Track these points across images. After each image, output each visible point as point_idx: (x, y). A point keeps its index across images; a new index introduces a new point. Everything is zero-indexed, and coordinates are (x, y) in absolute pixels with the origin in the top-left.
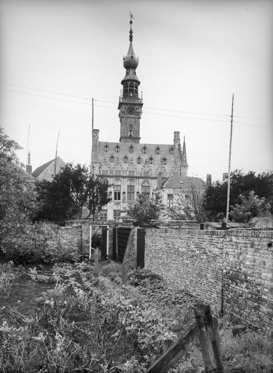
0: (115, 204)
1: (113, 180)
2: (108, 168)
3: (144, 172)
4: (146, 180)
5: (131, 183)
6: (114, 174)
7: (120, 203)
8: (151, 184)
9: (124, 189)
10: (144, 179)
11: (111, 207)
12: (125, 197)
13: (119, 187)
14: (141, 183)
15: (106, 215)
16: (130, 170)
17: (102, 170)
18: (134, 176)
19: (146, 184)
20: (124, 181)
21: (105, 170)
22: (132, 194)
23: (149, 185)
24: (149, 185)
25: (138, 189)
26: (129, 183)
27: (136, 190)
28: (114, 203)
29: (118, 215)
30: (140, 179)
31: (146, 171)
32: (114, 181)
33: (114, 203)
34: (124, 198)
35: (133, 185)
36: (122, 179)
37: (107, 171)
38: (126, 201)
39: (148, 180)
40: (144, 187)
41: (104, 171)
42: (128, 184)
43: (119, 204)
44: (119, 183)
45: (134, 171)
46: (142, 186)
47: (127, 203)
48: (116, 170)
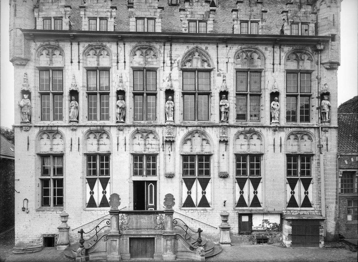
0: (91, 132)
1: (82, 49)
2: (62, 10)
3: (190, 21)
4: (197, 49)
5: (146, 62)
6: (85, 27)
7: (106, 129)
8: (216, 63)
9: (121, 81)
10: (191, 46)
11: (75, 146)
12: (123, 109)
13: (104, 75)
14: (180, 59)
15: (60, 171)
16: (139, 14)
17: (42, 14)
18: (155, 33)
19: (197, 64)
20: (121, 54)
21: (53, 14)
22: (151, 99)
23: (206, 66)
24: (209, 65)
25: (170, 80)
26: (138, 61)
27: (163, 85)
28: (86, 130)
29: (102, 173)
30: (174, 46)
31: (197, 17)
32: (86, 53)
33: (86, 130)
34: (118, 110)
35: (154, 65)
36: (112, 47)
37: (60, 18)
38: (129, 121)
39: (203, 47)
40: (189, 74)
41: (50, 19)
42: (136, 65)
43: (105, 132)
44: (104, 62)
45: (154, 19)
46: (184, 70)
47: (133, 129)
48: (91, 15)
